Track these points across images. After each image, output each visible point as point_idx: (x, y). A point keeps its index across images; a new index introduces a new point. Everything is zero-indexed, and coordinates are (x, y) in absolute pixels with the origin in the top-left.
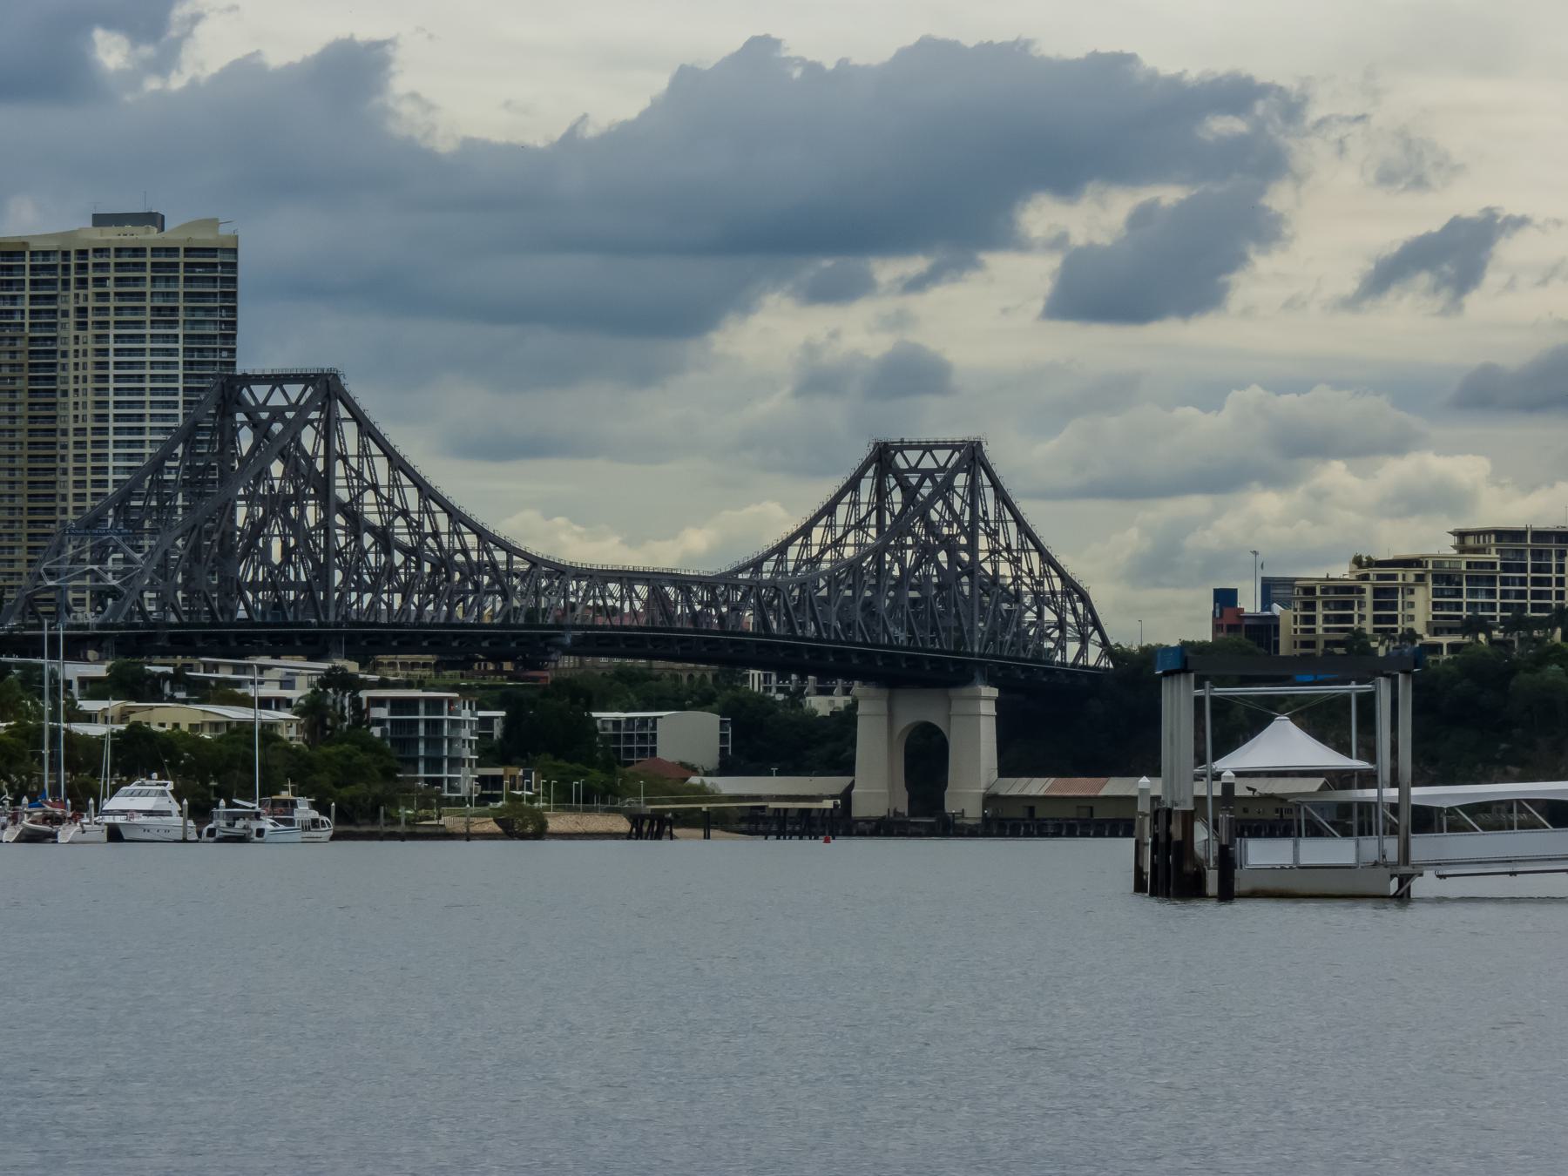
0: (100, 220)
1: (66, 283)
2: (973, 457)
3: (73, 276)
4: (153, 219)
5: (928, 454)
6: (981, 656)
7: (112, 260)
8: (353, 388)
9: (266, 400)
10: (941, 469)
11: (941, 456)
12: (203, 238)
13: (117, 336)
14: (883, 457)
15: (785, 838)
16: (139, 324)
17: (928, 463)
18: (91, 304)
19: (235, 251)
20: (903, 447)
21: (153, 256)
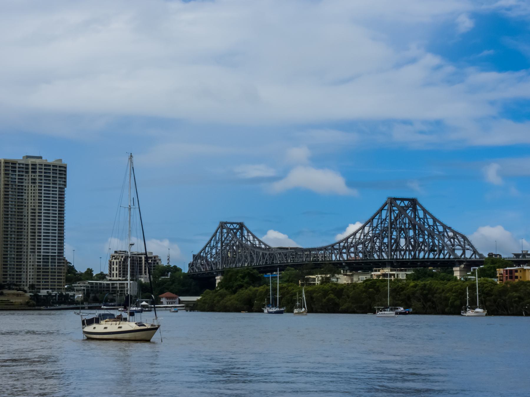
0: (28, 157)
1: (27, 172)
2: (242, 226)
3: (30, 170)
4: (41, 158)
5: (232, 225)
6: (222, 269)
7: (43, 167)
8: (421, 201)
9: (401, 202)
10: (235, 229)
11: (235, 225)
12: (58, 163)
13: (44, 186)
14: (222, 225)
15: (192, 311)
16: (49, 184)
17: (232, 227)
18: (37, 178)
19: (65, 168)
20: (226, 223)
21: (44, 166)
